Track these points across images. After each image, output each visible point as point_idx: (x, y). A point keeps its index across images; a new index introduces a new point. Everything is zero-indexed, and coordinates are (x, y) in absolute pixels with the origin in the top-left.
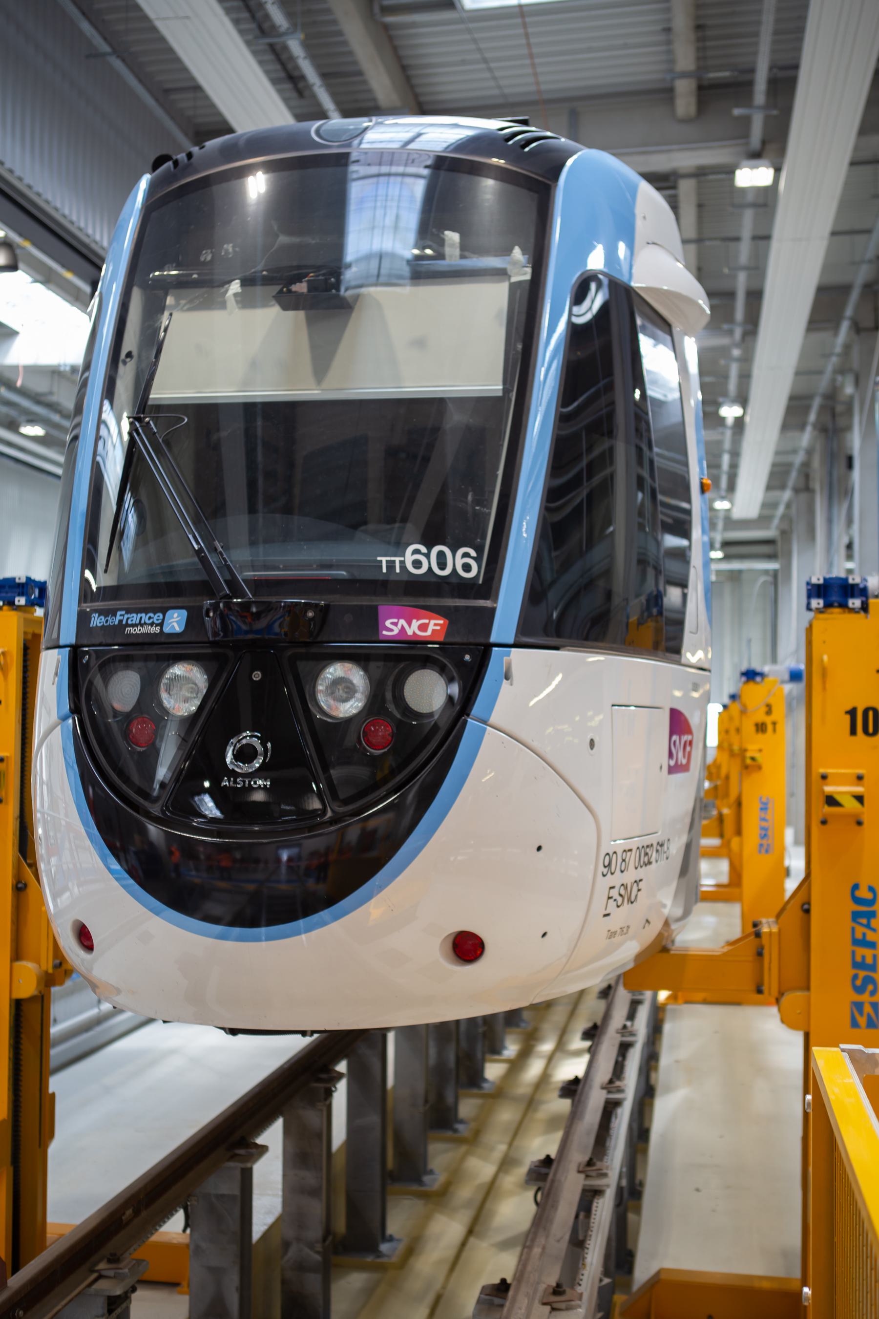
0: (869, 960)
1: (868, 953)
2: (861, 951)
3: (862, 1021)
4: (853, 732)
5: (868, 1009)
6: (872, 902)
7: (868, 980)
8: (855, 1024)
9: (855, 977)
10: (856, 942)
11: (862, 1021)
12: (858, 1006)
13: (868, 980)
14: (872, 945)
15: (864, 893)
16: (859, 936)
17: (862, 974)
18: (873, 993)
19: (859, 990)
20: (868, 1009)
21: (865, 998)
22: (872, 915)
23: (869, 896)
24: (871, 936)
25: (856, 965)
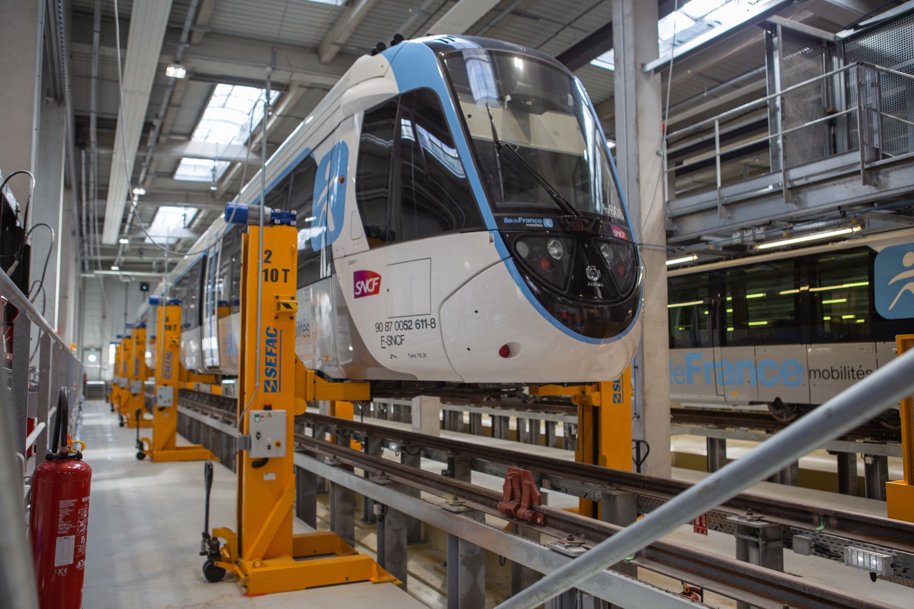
0: (273, 362)
1: (273, 358)
2: (269, 358)
3: (270, 389)
4: (266, 280)
5: (272, 383)
6: (275, 336)
7: (273, 370)
8: (266, 390)
9: (267, 369)
10: (268, 353)
11: (270, 389)
12: (268, 382)
13: (273, 370)
14: (275, 355)
15: (271, 332)
16: (269, 350)
17: (270, 368)
18: (274, 376)
19: (268, 375)
20: (272, 383)
21: (271, 378)
22: (276, 341)
23: (274, 333)
24: (274, 351)
25: (267, 364)
